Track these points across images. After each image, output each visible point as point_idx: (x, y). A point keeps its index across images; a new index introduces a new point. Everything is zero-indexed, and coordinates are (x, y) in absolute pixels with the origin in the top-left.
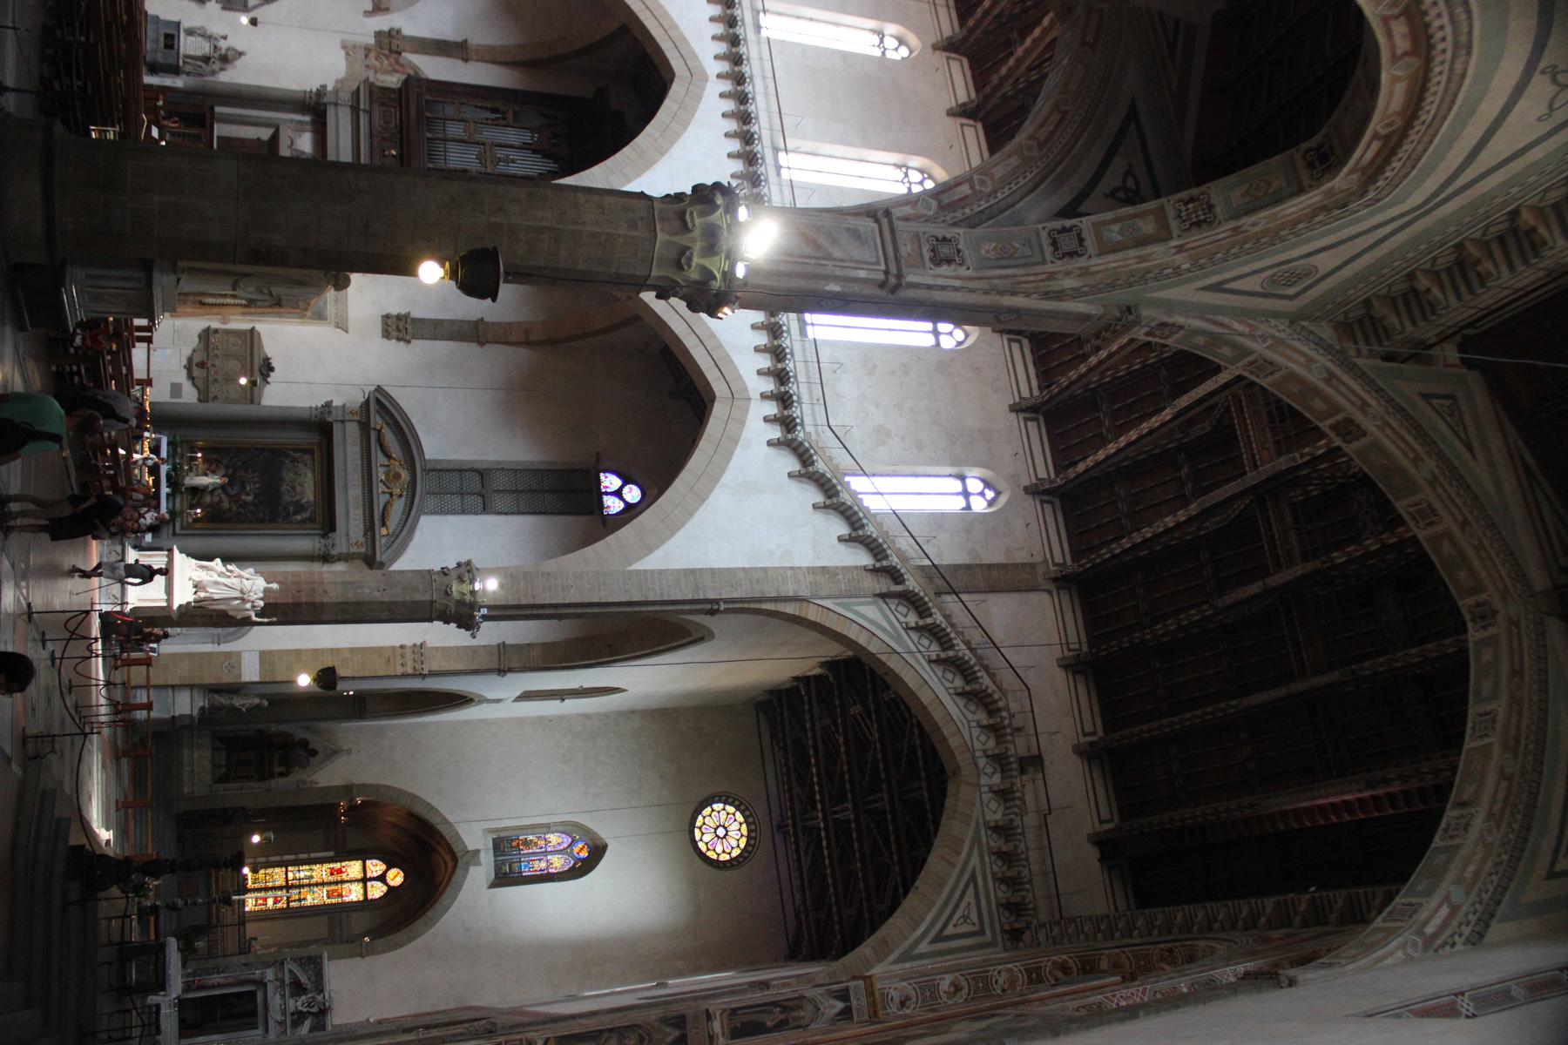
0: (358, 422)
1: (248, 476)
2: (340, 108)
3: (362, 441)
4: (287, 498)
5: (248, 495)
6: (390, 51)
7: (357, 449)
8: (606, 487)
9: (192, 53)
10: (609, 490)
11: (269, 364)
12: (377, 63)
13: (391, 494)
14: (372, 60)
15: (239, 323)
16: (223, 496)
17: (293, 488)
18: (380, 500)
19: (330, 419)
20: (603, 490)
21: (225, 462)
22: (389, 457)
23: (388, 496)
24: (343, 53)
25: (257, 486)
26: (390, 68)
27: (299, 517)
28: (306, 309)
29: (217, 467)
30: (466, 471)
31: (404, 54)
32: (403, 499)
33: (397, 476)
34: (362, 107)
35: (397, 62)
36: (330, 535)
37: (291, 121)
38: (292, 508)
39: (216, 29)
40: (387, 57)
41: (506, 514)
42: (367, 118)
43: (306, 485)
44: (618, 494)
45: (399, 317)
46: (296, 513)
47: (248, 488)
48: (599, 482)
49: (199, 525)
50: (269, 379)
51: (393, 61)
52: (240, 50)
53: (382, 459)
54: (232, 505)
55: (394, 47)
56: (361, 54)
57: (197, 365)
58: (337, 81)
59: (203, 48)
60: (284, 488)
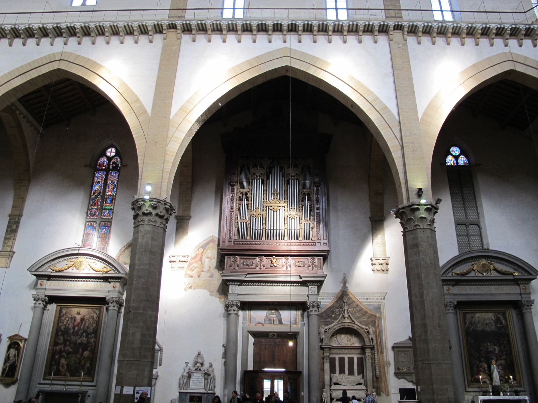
1: (484, 349)
3: (462, 285)
4: (493, 328)
5: (495, 349)
7: (468, 287)
8: (454, 162)
15: (390, 356)
17: (487, 324)
18: (494, 275)
20: (456, 164)
21: (477, 363)
25: (489, 344)
26: (199, 262)
27: (503, 321)
28: (375, 316)
29: (481, 367)
33: (484, 266)
38: (499, 325)
39: (179, 370)
43: (484, 317)
46: (501, 323)
47: (491, 349)
49: (518, 376)
53: (472, 274)
54: (502, 358)
60: (488, 329)
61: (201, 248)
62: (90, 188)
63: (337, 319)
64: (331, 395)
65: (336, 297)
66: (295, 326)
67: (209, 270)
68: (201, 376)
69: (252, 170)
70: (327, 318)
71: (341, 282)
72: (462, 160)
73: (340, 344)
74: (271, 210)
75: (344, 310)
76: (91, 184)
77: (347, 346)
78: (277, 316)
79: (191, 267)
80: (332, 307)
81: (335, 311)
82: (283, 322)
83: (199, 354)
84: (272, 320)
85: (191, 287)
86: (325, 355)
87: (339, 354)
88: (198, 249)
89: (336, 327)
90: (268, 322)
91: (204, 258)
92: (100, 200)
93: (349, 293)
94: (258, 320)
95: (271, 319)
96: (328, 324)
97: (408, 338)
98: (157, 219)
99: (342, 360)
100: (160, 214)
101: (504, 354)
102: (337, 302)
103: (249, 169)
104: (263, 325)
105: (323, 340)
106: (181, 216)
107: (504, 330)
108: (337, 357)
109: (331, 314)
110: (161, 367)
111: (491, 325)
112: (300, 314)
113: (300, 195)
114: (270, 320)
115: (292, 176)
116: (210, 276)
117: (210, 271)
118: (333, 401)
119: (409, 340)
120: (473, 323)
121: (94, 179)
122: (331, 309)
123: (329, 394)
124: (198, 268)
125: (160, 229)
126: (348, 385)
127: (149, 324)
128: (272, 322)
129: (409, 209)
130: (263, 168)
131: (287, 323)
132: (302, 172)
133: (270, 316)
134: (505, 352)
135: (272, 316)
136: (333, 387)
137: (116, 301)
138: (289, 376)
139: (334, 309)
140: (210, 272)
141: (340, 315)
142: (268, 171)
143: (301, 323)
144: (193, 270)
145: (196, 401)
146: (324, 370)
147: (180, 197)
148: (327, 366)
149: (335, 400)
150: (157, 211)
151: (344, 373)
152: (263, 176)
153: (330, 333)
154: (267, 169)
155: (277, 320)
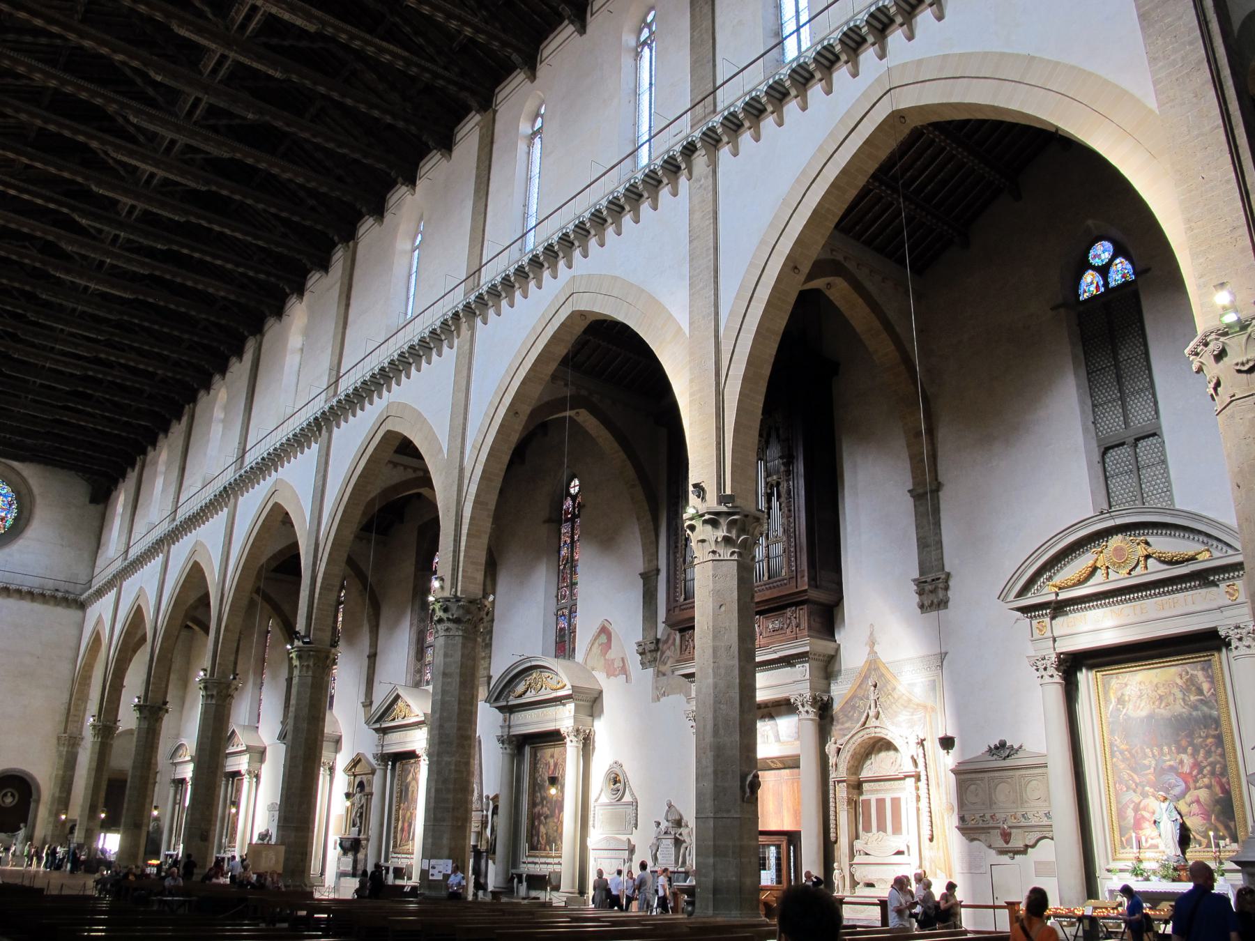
0: (1053, 618)
5: (1181, 762)
6: (657, 650)
10: (1101, 283)
11: (996, 748)
13: (1147, 557)
16: (1188, 798)
19: (1054, 658)
21: (1136, 799)
22: (1095, 569)
23: (1150, 561)
24: (662, 699)
25: (1166, 749)
26: (673, 647)
27: (1205, 686)
30: (1105, 470)
31: (659, 637)
32: (1150, 539)
33: (1118, 551)
35: (666, 641)
36: (1222, 633)
38: (1193, 698)
40: (663, 653)
41: (1156, 403)
44: (1104, 271)
45: (921, 593)
46: (1200, 691)
48: (1093, 298)
50: (1016, 747)
53: (1099, 576)
54: (1200, 784)
57: (1007, 842)
62: (557, 555)
64: (852, 876)
71: (866, 644)
72: (1090, 284)
76: (557, 549)
83: (670, 806)
92: (569, 572)
97: (986, 749)
101: (1205, 772)
107: (1205, 709)
111: (1171, 698)
120: (1127, 698)
121: (560, 538)
125: (457, 638)
134: (1208, 768)
144: (665, 664)
149: (861, 884)
151: (885, 831)
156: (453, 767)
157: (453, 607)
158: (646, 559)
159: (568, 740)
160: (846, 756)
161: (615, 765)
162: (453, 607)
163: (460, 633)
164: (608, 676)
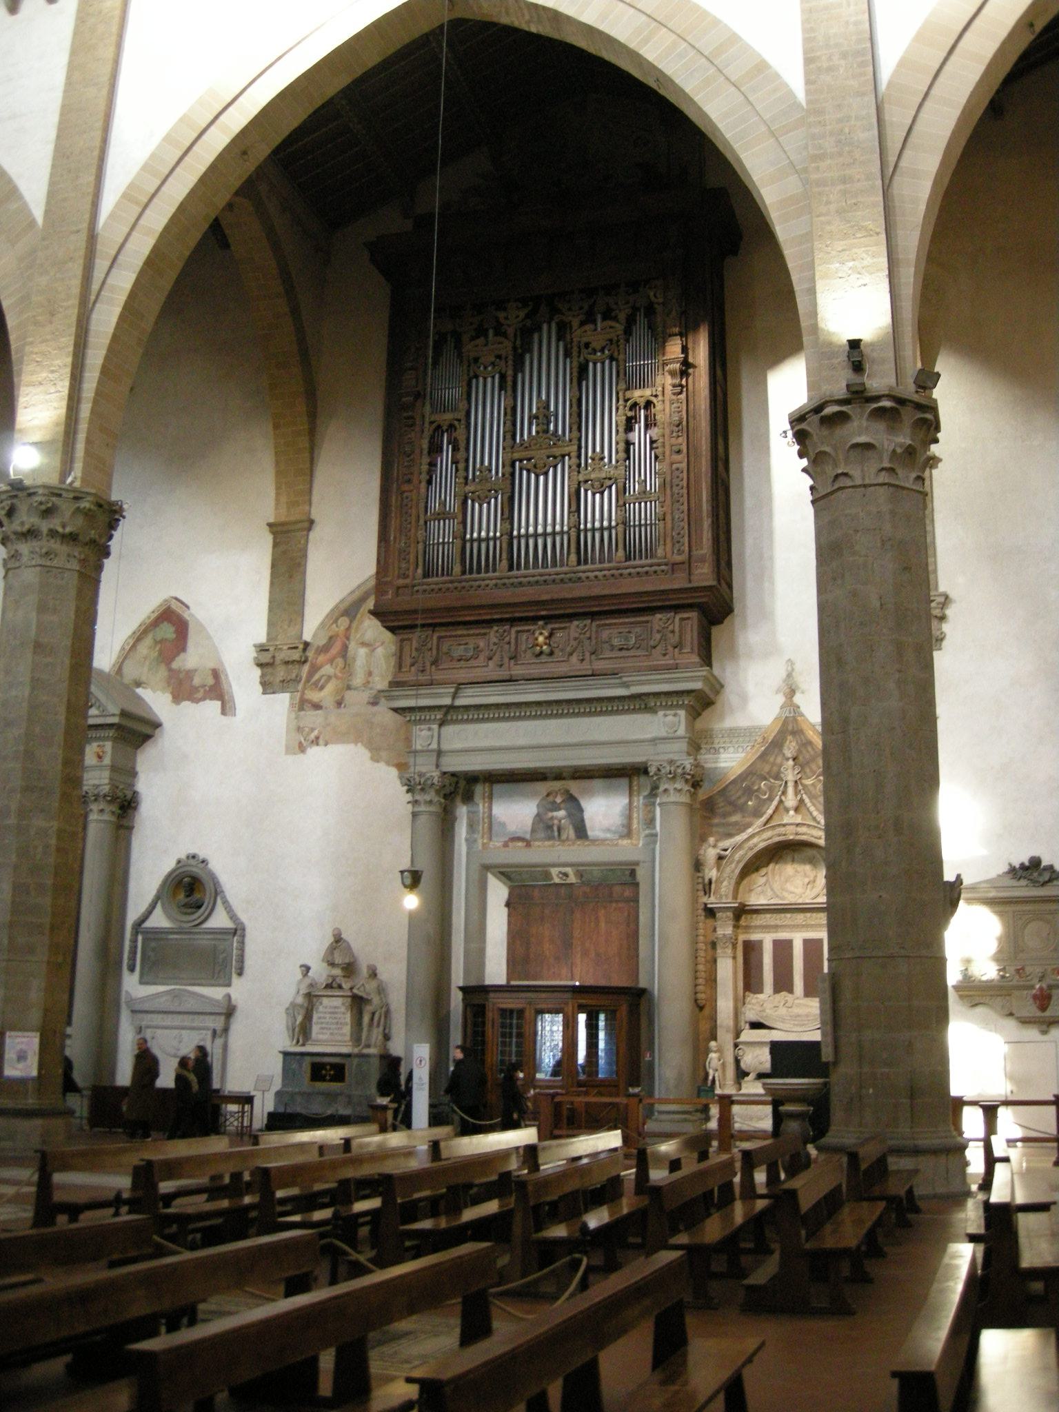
2: (444, 747)
9: (347, 1030)
12: (330, 687)
14: (326, 695)
24: (313, 751)
26: (340, 661)
31: (307, 636)
34: (447, 701)
37: (470, 842)
39: (288, 988)
40: (315, 669)
42: (469, 691)
51: (321, 658)
52: (332, 939)
55: (296, 655)
56: (312, 718)
57: (1043, 1008)
58: (375, 759)
59: (332, 1009)
61: (342, 615)
63: (761, 817)
64: (737, 1061)
65: (760, 740)
66: (625, 842)
67: (368, 682)
68: (343, 1004)
69: (469, 349)
70: (730, 814)
73: (777, 896)
74: (529, 471)
75: (786, 783)
77: (800, 901)
78: (570, 815)
79: (316, 677)
80: (747, 776)
81: (756, 788)
82: (590, 833)
84: (555, 828)
85: (317, 738)
86: (720, 932)
87: (776, 928)
88: (336, 621)
89: (755, 840)
90: (542, 835)
91: (352, 646)
93: (804, 727)
94: (512, 828)
95: (550, 823)
96: (733, 832)
97: (1006, 868)
98: (55, 545)
99: (782, 949)
100: (60, 530)
102: (763, 756)
103: (458, 345)
104: (528, 844)
105: (713, 886)
106: (282, 524)
108: (767, 941)
109: (742, 800)
110: (243, 979)
112: (641, 806)
113: (621, 411)
114: (549, 827)
115: (595, 352)
116: (371, 701)
117: (370, 685)
118: (746, 1079)
119: (1011, 875)
122: (743, 781)
123: (730, 1060)
124: (336, 676)
126: (795, 1029)
127: (38, 857)
128: (556, 834)
129: (815, 418)
130: (505, 335)
131: (601, 835)
132: (628, 332)
133: (550, 814)
135: (555, 814)
136: (748, 1035)
137: (105, 796)
138: (580, 1001)
139: (753, 784)
140: (371, 689)
141: (771, 799)
142: (518, 342)
143: (647, 832)
144: (322, 688)
145: (328, 1078)
146: (715, 980)
147: (277, 463)
148: (727, 969)
149: (752, 1076)
150: (55, 523)
151: (790, 990)
152: (503, 363)
153: (739, 862)
154: (515, 335)
155: (571, 827)
156: (53, 842)
157: (67, 508)
158: (284, 499)
159: (94, 807)
160: (733, 869)
161: (192, 862)
162: (67, 508)
163: (75, 565)
164: (177, 698)
